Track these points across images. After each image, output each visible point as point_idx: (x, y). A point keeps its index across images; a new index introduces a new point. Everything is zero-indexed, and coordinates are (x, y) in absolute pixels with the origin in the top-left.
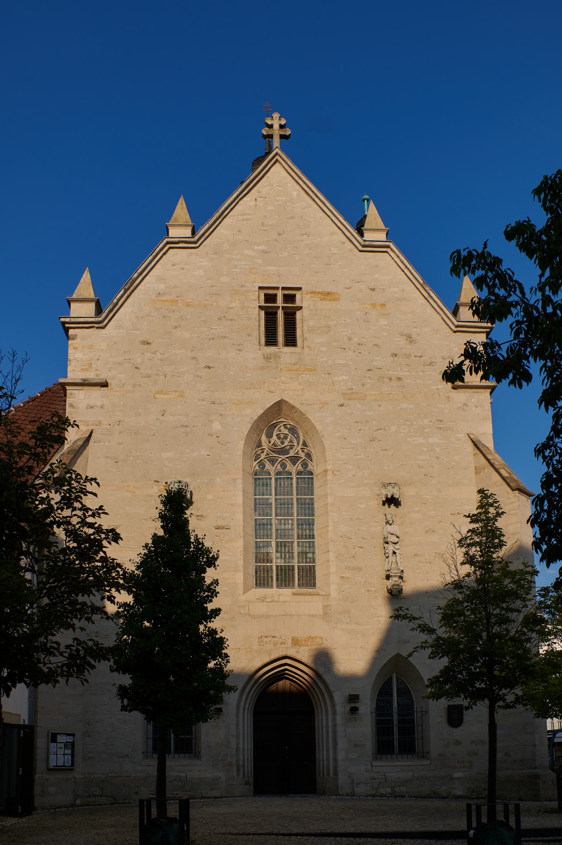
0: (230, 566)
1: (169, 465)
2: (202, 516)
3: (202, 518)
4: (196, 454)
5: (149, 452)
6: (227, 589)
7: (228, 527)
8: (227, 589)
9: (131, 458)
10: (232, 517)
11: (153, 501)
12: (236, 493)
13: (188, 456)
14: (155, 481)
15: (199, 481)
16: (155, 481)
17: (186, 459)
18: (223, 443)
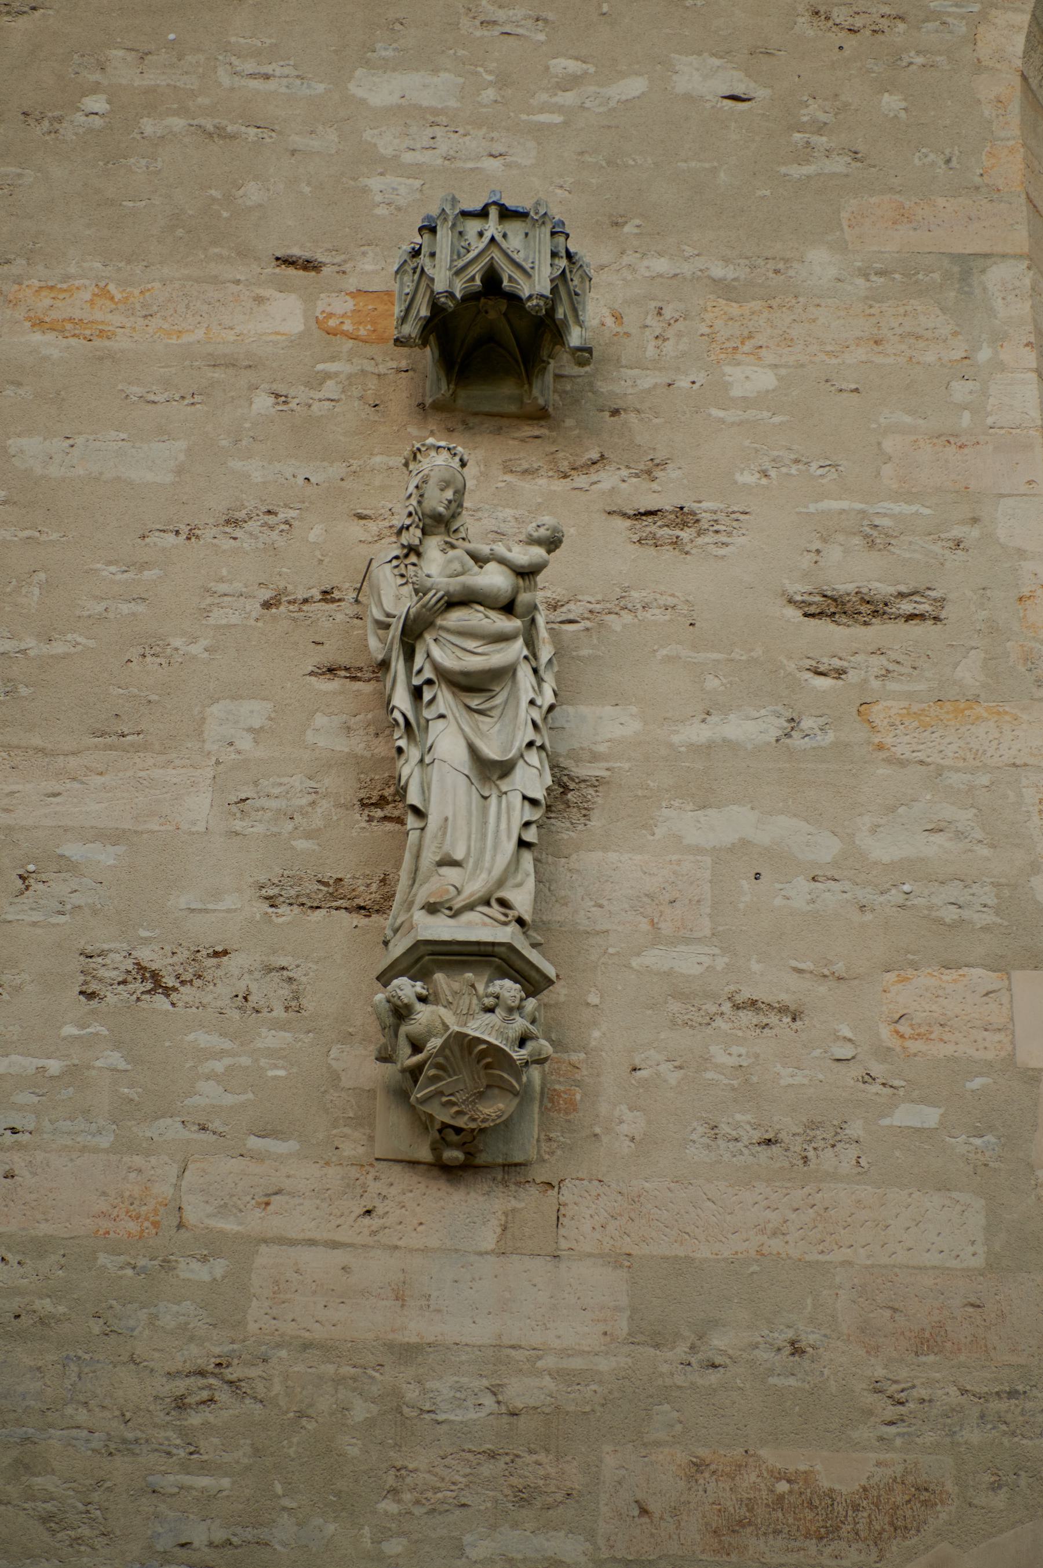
0: (950, 914)
1: (408, 157)
2: (684, 517)
3: (685, 535)
4: (634, 86)
5: (250, 66)
6: (930, 1116)
7: (925, 607)
8: (930, 1116)
9: (97, 103)
10: (957, 532)
11: (263, 402)
12: (984, 355)
13: (568, 98)
14: (288, 262)
15: (662, 265)
16: (288, 262)
17: (557, 119)
18: (858, 22)
